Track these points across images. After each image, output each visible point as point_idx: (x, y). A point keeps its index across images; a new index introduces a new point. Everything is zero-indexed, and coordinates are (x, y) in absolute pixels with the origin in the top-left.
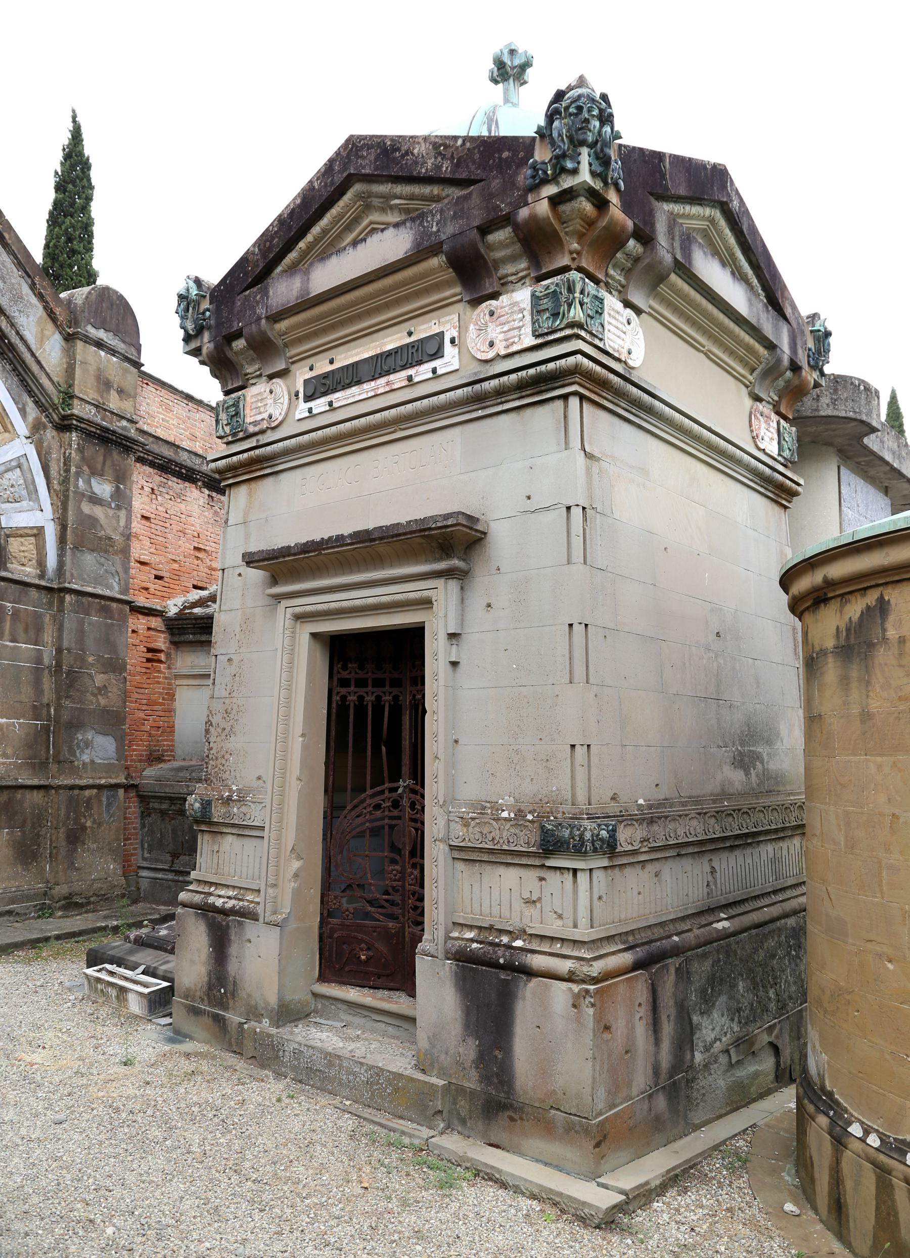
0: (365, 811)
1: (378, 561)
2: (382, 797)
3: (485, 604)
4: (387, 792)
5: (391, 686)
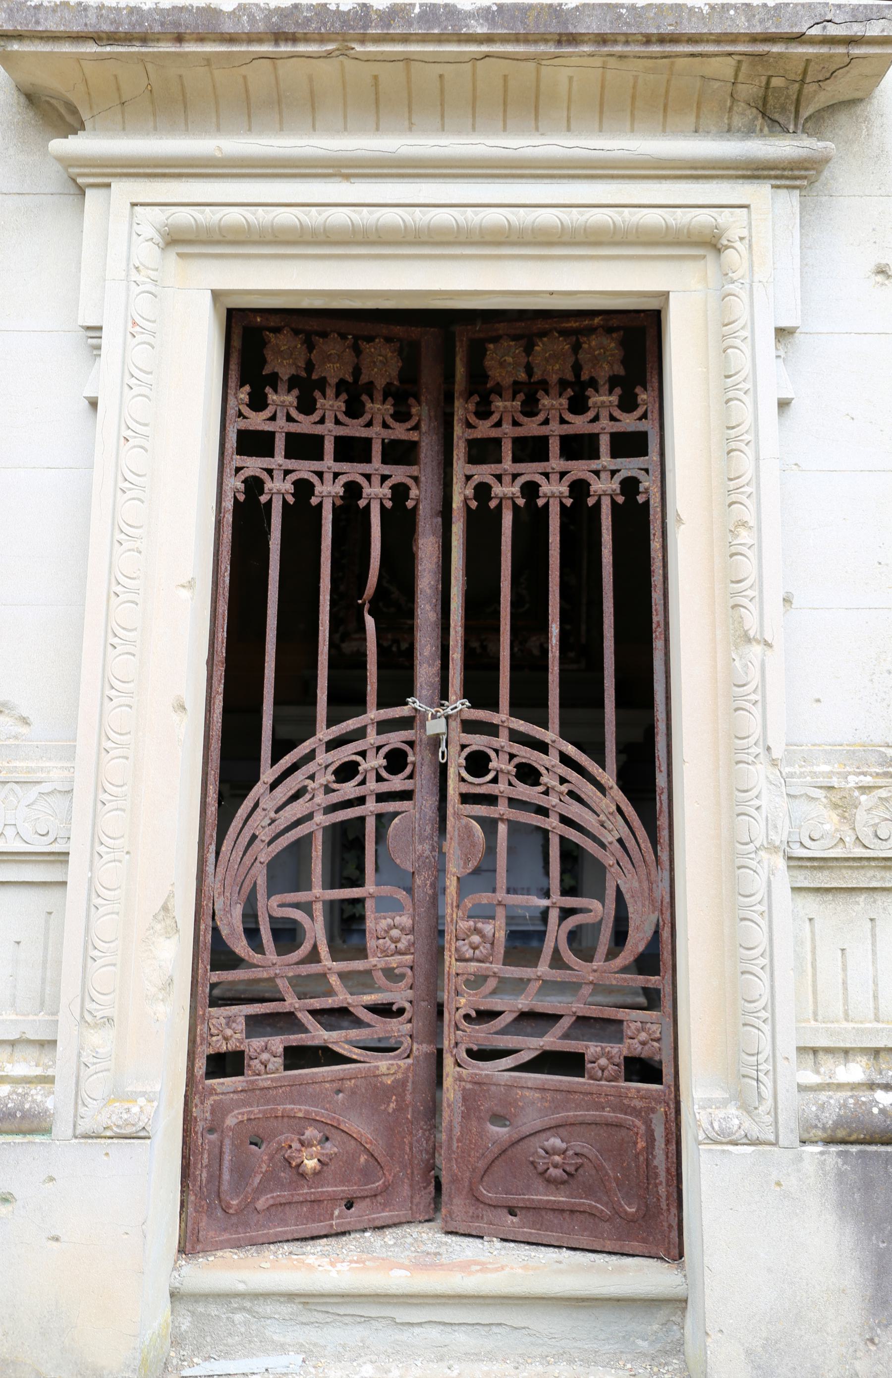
0: (311, 785)
1: (528, 105)
2: (359, 746)
3: (872, 266)
4: (371, 731)
5: (614, 455)
